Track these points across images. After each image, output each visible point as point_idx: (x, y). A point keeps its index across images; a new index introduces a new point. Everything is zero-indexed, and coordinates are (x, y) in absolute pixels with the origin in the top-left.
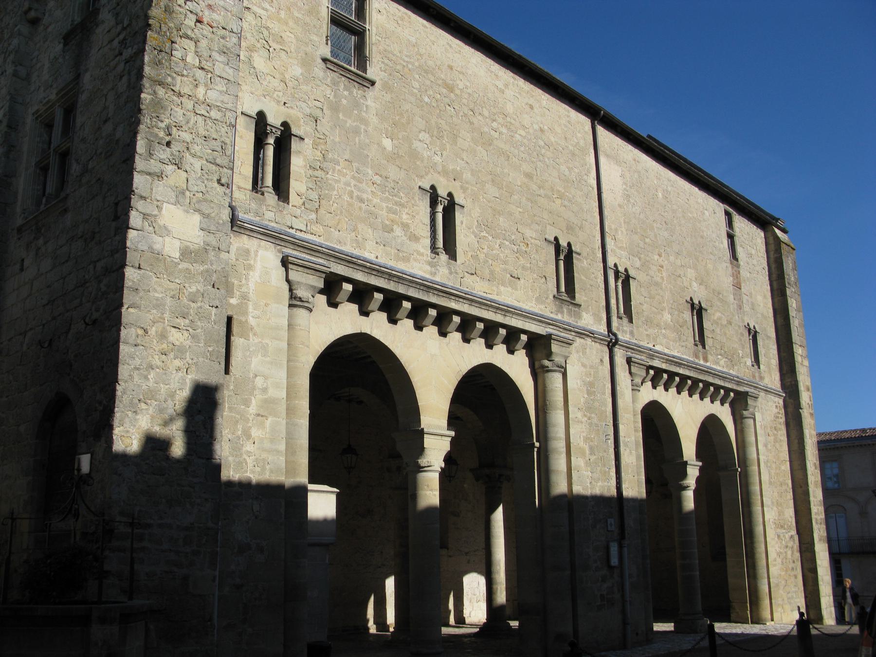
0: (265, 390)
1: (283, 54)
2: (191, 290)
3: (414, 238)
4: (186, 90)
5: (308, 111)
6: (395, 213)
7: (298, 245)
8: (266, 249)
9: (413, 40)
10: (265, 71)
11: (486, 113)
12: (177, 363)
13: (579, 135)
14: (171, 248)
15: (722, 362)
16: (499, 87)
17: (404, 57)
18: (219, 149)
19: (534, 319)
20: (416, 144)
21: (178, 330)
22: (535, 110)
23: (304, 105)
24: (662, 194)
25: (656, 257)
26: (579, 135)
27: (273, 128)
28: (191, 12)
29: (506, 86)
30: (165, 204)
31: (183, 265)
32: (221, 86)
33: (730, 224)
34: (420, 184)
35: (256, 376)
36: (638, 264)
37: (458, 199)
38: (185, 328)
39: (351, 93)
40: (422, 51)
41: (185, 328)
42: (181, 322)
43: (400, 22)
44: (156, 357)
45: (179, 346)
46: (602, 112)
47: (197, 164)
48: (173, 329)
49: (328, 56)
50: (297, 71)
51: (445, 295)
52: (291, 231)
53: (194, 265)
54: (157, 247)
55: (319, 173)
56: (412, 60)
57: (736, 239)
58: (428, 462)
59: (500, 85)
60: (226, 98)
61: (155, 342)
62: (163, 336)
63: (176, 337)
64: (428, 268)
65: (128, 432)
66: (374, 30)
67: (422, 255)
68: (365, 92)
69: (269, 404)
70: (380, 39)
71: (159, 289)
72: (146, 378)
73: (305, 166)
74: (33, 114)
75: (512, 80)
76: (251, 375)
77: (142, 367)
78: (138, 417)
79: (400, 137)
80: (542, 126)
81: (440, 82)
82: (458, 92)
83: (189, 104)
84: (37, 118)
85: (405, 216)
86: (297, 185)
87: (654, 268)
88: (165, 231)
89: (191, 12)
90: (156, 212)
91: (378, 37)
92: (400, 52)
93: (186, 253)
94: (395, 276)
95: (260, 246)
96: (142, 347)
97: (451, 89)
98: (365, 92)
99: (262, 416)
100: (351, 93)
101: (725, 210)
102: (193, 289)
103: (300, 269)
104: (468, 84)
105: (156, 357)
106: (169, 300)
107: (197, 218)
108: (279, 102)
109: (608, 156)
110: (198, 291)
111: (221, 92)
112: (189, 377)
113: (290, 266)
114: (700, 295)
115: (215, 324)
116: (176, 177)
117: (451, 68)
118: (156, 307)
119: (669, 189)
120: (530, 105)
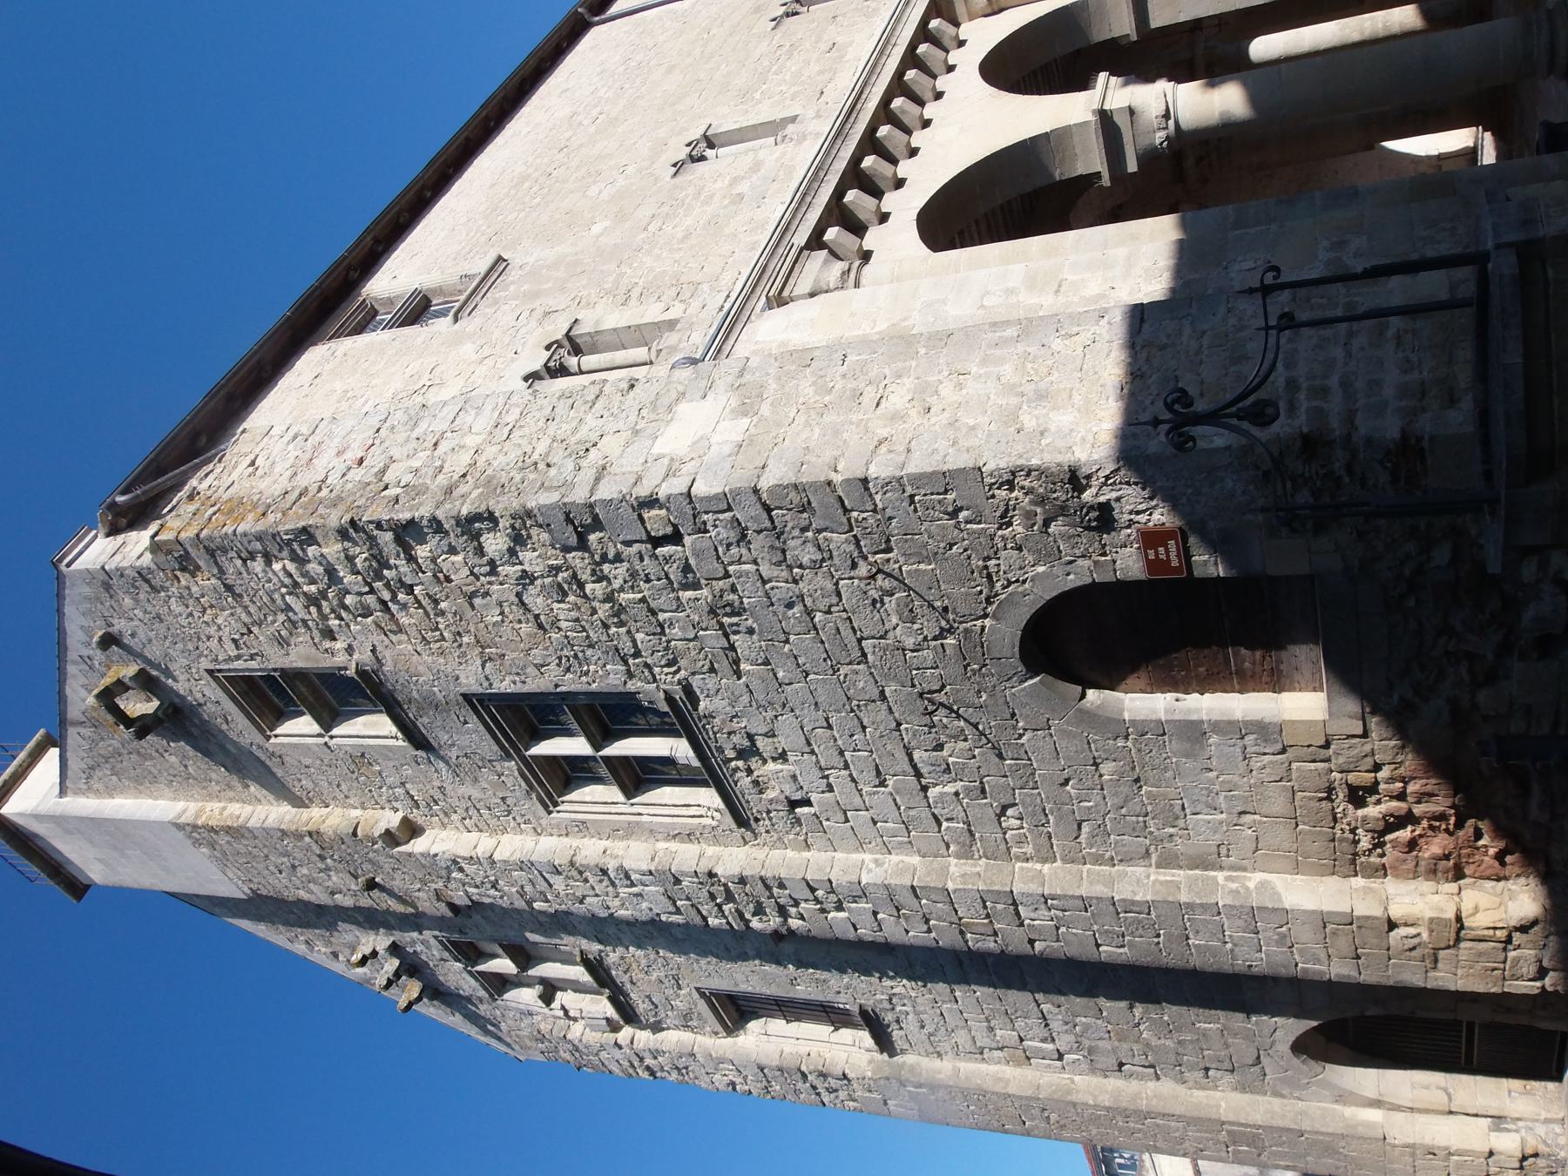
0: (1010, 292)
1: (437, 371)
2: (811, 393)
3: (757, 166)
4: (465, 459)
5: (533, 324)
6: (712, 197)
7: (751, 293)
10: (462, 383)
11: (567, 135)
12: (947, 390)
14: (734, 430)
18: (571, 401)
19: (903, 11)
20: (605, 195)
21: (885, 399)
23: (523, 331)
27: (554, 358)
28: (344, 475)
30: (652, 451)
31: (765, 409)
32: (467, 418)
34: (668, 178)
35: (982, 306)
37: (697, 133)
38: (881, 391)
39: (513, 283)
41: (881, 391)
42: (870, 396)
44: (933, 421)
45: (915, 393)
46: (579, 10)
47: (591, 421)
48: (882, 406)
49: (450, 317)
50: (468, 349)
51: (854, 115)
52: (725, 310)
53: (765, 396)
54: (727, 449)
55: (635, 294)
58: (1157, 98)
60: (488, 408)
61: (904, 425)
62: (896, 417)
63: (897, 399)
64: (806, 143)
65: (1083, 439)
67: (784, 154)
69: (1032, 283)
71: (804, 436)
72: (973, 428)
73: (620, 311)
75: (522, 119)
76: (982, 312)
77: (952, 437)
78: (1053, 428)
79: (590, 216)
81: (513, 192)
82: (530, 171)
83: (491, 451)
85: (719, 184)
86: (652, 313)
88: (702, 444)
89: (344, 475)
90: (666, 461)
93: (744, 410)
94: (816, 173)
96: (913, 443)
97: (524, 178)
99: (1060, 286)
100: (513, 283)
102: (811, 391)
103: (791, 281)
105: (933, 421)
106: (830, 418)
107: (683, 408)
108: (513, 360)
110: (814, 383)
111: (477, 414)
112: (974, 370)
113: (785, 293)
115: (874, 353)
116: (611, 446)
118: (836, 433)
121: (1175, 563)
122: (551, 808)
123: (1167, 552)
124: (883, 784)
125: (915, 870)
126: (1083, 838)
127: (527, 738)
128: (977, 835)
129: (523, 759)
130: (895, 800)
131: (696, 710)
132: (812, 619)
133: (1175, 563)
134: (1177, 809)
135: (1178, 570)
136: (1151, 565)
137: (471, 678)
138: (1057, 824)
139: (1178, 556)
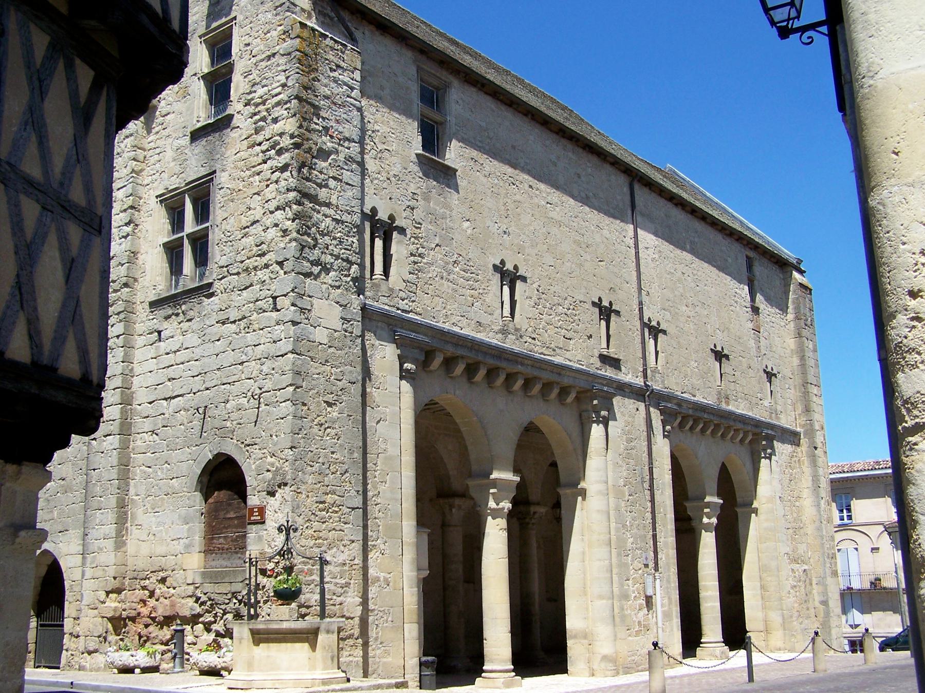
8: (382, 329)
9: (483, 124)
13: (619, 198)
15: (742, 406)
16: (552, 160)
17: (478, 143)
22: (583, 178)
24: (690, 246)
25: (685, 308)
26: (619, 198)
29: (558, 158)
33: (750, 267)
36: (668, 316)
40: (492, 134)
43: (473, 110)
56: (484, 145)
57: (756, 282)
59: (553, 158)
66: (453, 121)
68: (448, 180)
70: (459, 129)
74: (157, 197)
80: (587, 193)
84: (161, 202)
87: (683, 319)
91: (456, 127)
92: (474, 138)
95: (377, 327)
98: (448, 180)
101: (747, 257)
104: (528, 161)
109: (643, 215)
114: (721, 341)
117: (513, 147)
119: (696, 240)
120: (578, 174)
121: (252, 518)
122: (159, 199)
123: (256, 516)
124: (169, 380)
125: (129, 389)
126: (143, 468)
127: (194, 195)
128: (145, 420)
129: (184, 192)
130: (161, 384)
131: (204, 296)
132: (239, 364)
133: (252, 518)
134: (157, 510)
135: (249, 519)
136: (251, 511)
137: (222, 178)
138: (150, 457)
139: (255, 520)
